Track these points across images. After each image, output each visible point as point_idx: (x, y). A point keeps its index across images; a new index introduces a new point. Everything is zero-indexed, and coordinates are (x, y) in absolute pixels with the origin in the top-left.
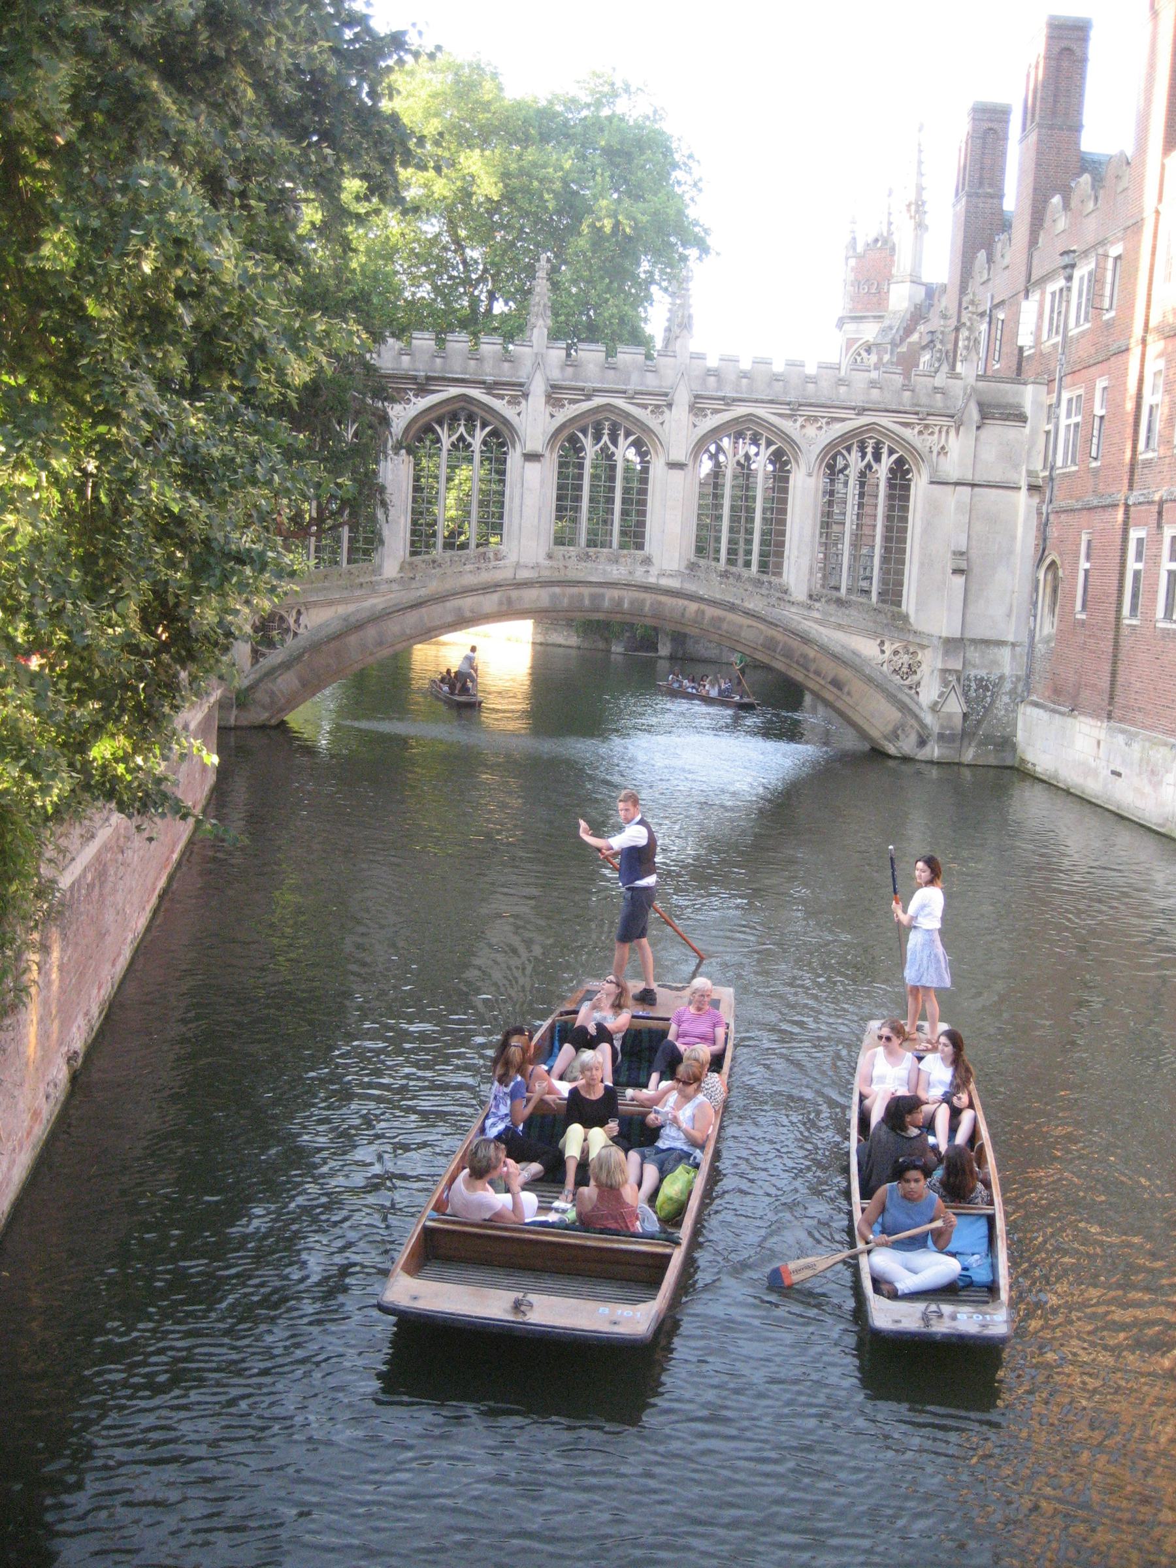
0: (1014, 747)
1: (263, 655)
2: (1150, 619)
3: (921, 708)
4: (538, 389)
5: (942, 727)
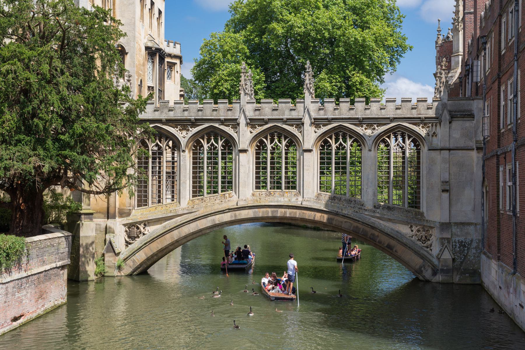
0: (480, 275)
1: (130, 244)
3: (433, 257)
5: (442, 265)
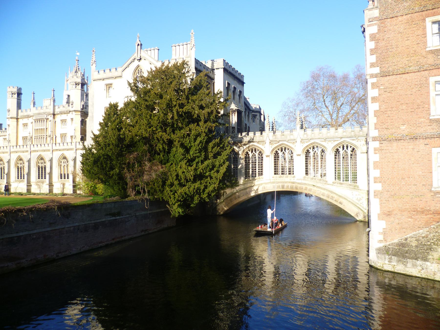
4: (268, 142)
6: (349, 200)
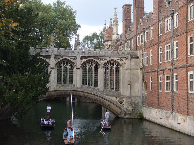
1: (3, 107)
2: (164, 91)
4: (53, 57)
6: (114, 103)
